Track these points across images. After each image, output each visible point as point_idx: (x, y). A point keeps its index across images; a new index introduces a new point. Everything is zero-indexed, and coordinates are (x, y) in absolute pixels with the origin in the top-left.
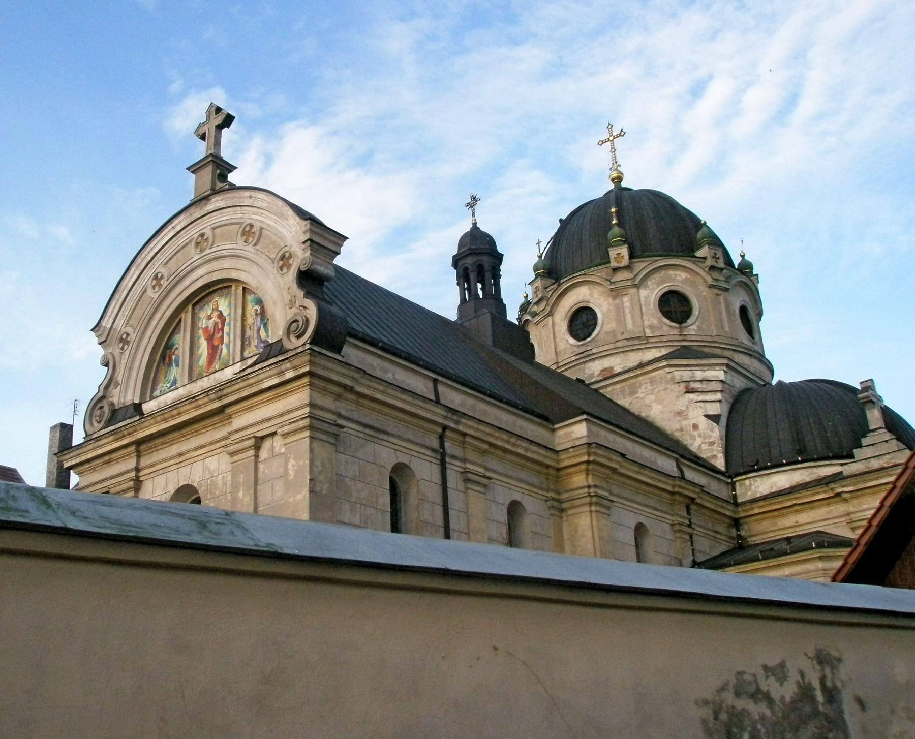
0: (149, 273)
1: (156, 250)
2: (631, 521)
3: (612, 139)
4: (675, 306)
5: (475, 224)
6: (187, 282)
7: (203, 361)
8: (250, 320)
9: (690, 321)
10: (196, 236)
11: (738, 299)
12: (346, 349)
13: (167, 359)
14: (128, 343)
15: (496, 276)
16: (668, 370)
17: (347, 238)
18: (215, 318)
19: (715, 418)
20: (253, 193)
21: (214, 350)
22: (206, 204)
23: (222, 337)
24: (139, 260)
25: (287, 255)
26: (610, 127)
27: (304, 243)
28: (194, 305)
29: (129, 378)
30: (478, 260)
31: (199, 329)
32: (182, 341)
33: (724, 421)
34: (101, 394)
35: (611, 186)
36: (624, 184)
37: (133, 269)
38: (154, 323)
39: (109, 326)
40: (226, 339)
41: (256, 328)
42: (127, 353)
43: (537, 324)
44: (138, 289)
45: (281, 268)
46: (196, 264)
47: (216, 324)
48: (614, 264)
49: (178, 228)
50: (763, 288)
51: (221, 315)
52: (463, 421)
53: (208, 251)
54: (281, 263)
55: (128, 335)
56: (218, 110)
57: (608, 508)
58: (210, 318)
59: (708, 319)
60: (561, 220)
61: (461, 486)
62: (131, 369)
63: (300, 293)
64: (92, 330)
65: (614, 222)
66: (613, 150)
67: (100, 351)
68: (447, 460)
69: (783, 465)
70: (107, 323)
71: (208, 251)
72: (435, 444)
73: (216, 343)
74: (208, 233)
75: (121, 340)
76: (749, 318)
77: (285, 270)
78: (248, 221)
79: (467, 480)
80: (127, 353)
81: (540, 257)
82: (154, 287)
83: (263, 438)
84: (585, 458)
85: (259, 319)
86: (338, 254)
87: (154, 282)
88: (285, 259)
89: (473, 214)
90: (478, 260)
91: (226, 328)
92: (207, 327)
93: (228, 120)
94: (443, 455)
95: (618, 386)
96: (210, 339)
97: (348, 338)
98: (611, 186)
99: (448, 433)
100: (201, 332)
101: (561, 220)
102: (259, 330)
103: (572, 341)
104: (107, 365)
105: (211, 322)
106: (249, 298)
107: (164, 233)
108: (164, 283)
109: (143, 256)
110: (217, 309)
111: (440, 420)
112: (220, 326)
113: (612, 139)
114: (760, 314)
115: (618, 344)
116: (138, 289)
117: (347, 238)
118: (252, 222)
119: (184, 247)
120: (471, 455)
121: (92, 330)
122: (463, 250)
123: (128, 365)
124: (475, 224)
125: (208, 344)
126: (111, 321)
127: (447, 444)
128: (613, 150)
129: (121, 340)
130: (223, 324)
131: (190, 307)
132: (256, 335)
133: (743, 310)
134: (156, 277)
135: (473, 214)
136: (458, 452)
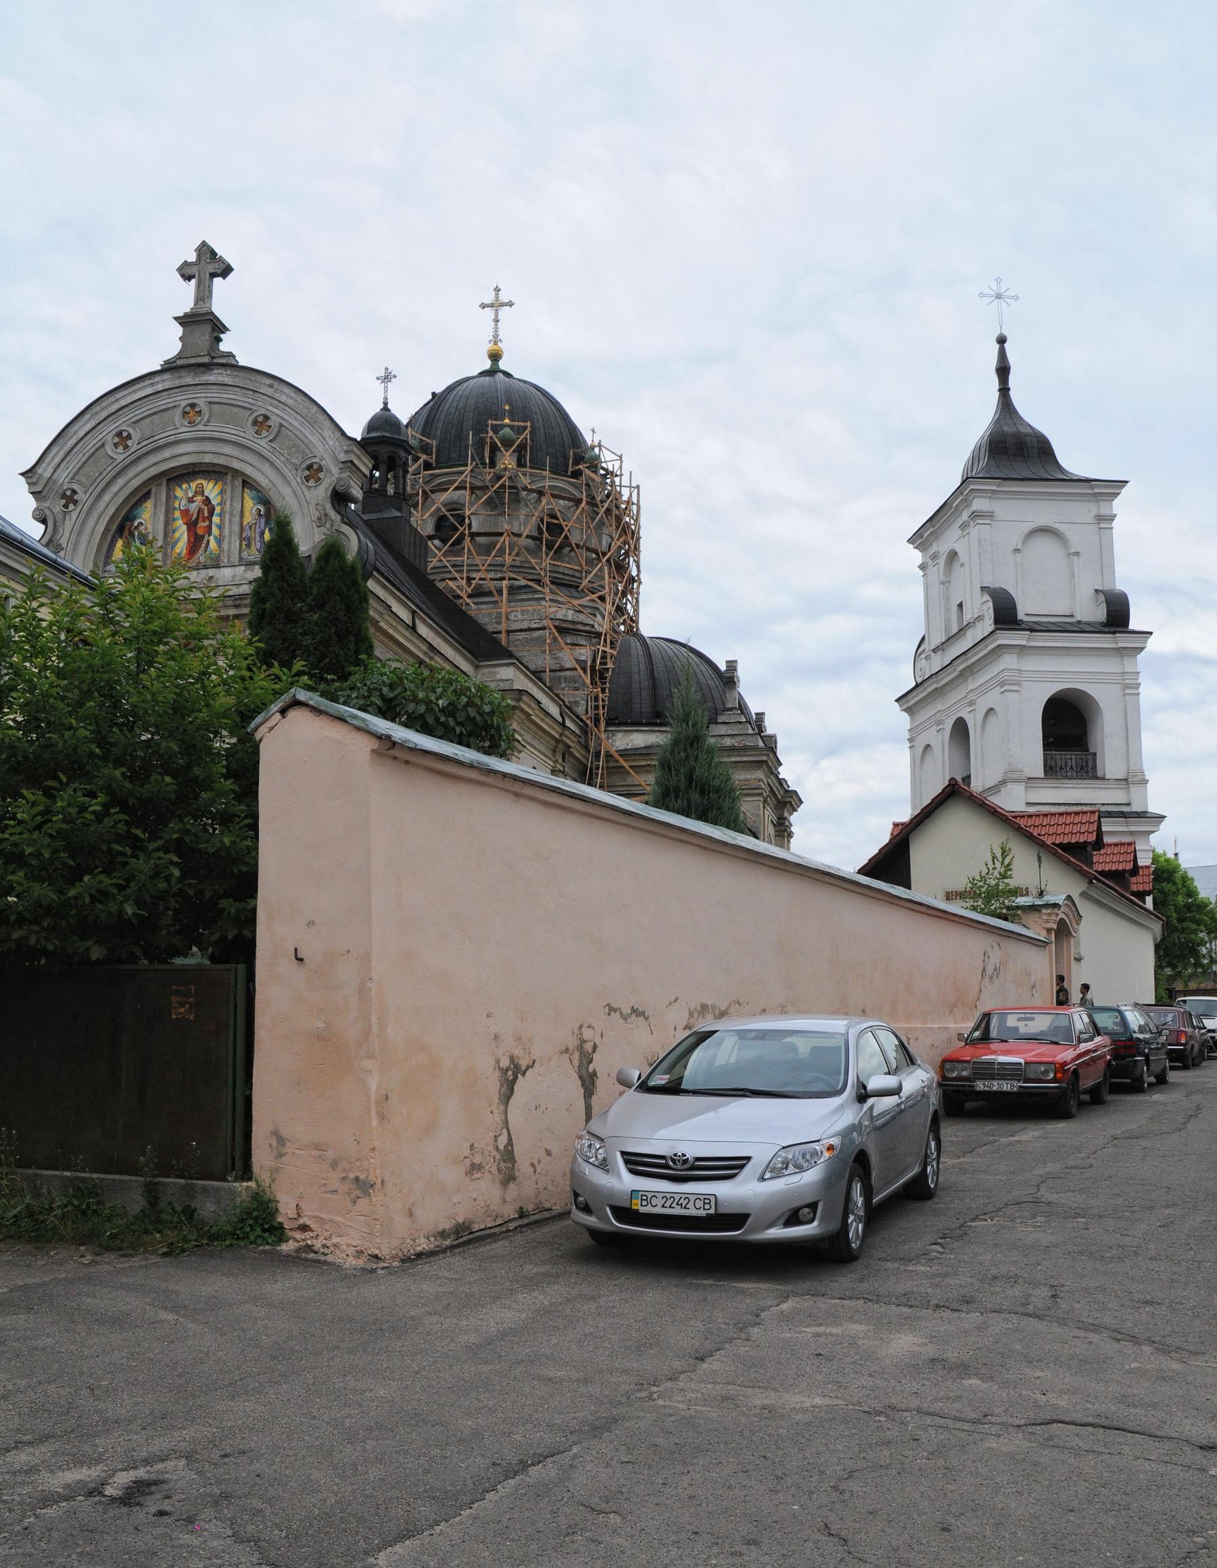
0: (111, 428)
1: (123, 403)
3: (497, 305)
5: (386, 408)
6: (167, 453)
7: (182, 546)
10: (183, 404)
13: (126, 532)
14: (75, 502)
20: (276, 384)
21: (196, 541)
22: (204, 373)
23: (210, 527)
25: (315, 467)
26: (497, 290)
28: (169, 480)
29: (76, 544)
31: (175, 509)
32: (149, 517)
35: (487, 364)
36: (502, 365)
37: (87, 416)
38: (115, 488)
39: (47, 475)
40: (215, 530)
41: (258, 530)
42: (74, 515)
44: (92, 442)
45: (307, 478)
46: (182, 436)
47: (200, 511)
49: (160, 387)
51: (207, 501)
52: (436, 658)
53: (201, 427)
54: (307, 473)
55: (74, 492)
58: (191, 500)
60: (434, 394)
62: (79, 534)
64: (23, 474)
66: (497, 321)
67: (31, 503)
69: (641, 724)
70: (45, 471)
71: (201, 427)
73: (200, 532)
74: (202, 404)
77: (312, 483)
78: (263, 412)
80: (74, 515)
82: (116, 445)
85: (263, 521)
87: (116, 440)
88: (313, 472)
89: (386, 391)
91: (216, 519)
92: (187, 511)
95: (485, 607)
96: (192, 526)
100: (177, 514)
101: (434, 394)
102: (262, 533)
104: (44, 521)
105: (193, 508)
107: (137, 387)
109: (104, 404)
110: (202, 493)
111: (422, 656)
113: (497, 305)
118: (269, 414)
119: (163, 411)
121: (23, 474)
122: (374, 434)
123: (77, 528)
124: (386, 408)
125: (189, 530)
126: (50, 470)
128: (497, 321)
129: (64, 496)
130: (211, 513)
131: (165, 483)
132: (258, 538)
134: (119, 434)
135: (386, 391)
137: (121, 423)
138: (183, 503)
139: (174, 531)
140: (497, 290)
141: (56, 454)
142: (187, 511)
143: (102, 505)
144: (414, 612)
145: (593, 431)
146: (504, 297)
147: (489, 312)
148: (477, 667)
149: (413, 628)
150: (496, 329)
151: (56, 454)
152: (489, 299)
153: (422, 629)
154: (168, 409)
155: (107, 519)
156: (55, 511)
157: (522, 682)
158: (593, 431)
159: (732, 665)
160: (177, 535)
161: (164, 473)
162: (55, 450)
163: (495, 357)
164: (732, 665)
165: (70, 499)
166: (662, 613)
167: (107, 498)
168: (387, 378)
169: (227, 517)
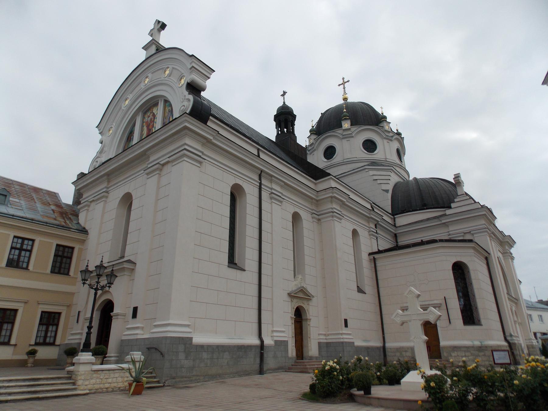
2: (351, 227)
3: (344, 83)
4: (369, 146)
5: (284, 103)
8: (166, 114)
9: (375, 152)
11: (395, 145)
12: (209, 123)
15: (293, 125)
16: (367, 170)
17: (214, 71)
18: (151, 117)
19: (387, 191)
26: (343, 79)
27: (191, 69)
30: (285, 118)
33: (390, 192)
35: (342, 102)
43: (310, 154)
47: (151, 119)
48: (343, 128)
50: (406, 142)
56: (159, 22)
57: (341, 219)
58: (149, 117)
59: (385, 151)
61: (269, 201)
63: (186, 93)
65: (345, 110)
66: (344, 88)
67: (100, 137)
68: (262, 186)
72: (257, 178)
73: (150, 128)
76: (400, 153)
78: (166, 66)
79: (271, 198)
81: (313, 127)
83: (163, 165)
84: (331, 195)
86: (209, 78)
90: (285, 118)
93: (163, 26)
94: (261, 184)
96: (148, 127)
97: (211, 117)
98: (342, 102)
99: (263, 174)
103: (325, 160)
104: (101, 143)
106: (167, 104)
113: (344, 83)
114: (404, 154)
115: (345, 161)
117: (214, 71)
120: (274, 186)
124: (284, 103)
127: (263, 182)
128: (344, 88)
130: (154, 119)
133: (398, 151)
136: (269, 185)
140: (343, 79)
144: (258, 150)
145: (382, 108)
146: (345, 80)
147: (342, 86)
148: (315, 184)
149: (259, 156)
150: (345, 91)
152: (341, 82)
153: (262, 156)
157: (334, 184)
158: (382, 108)
159: (457, 177)
163: (345, 99)
164: (457, 177)
166: (421, 165)
168: (285, 93)
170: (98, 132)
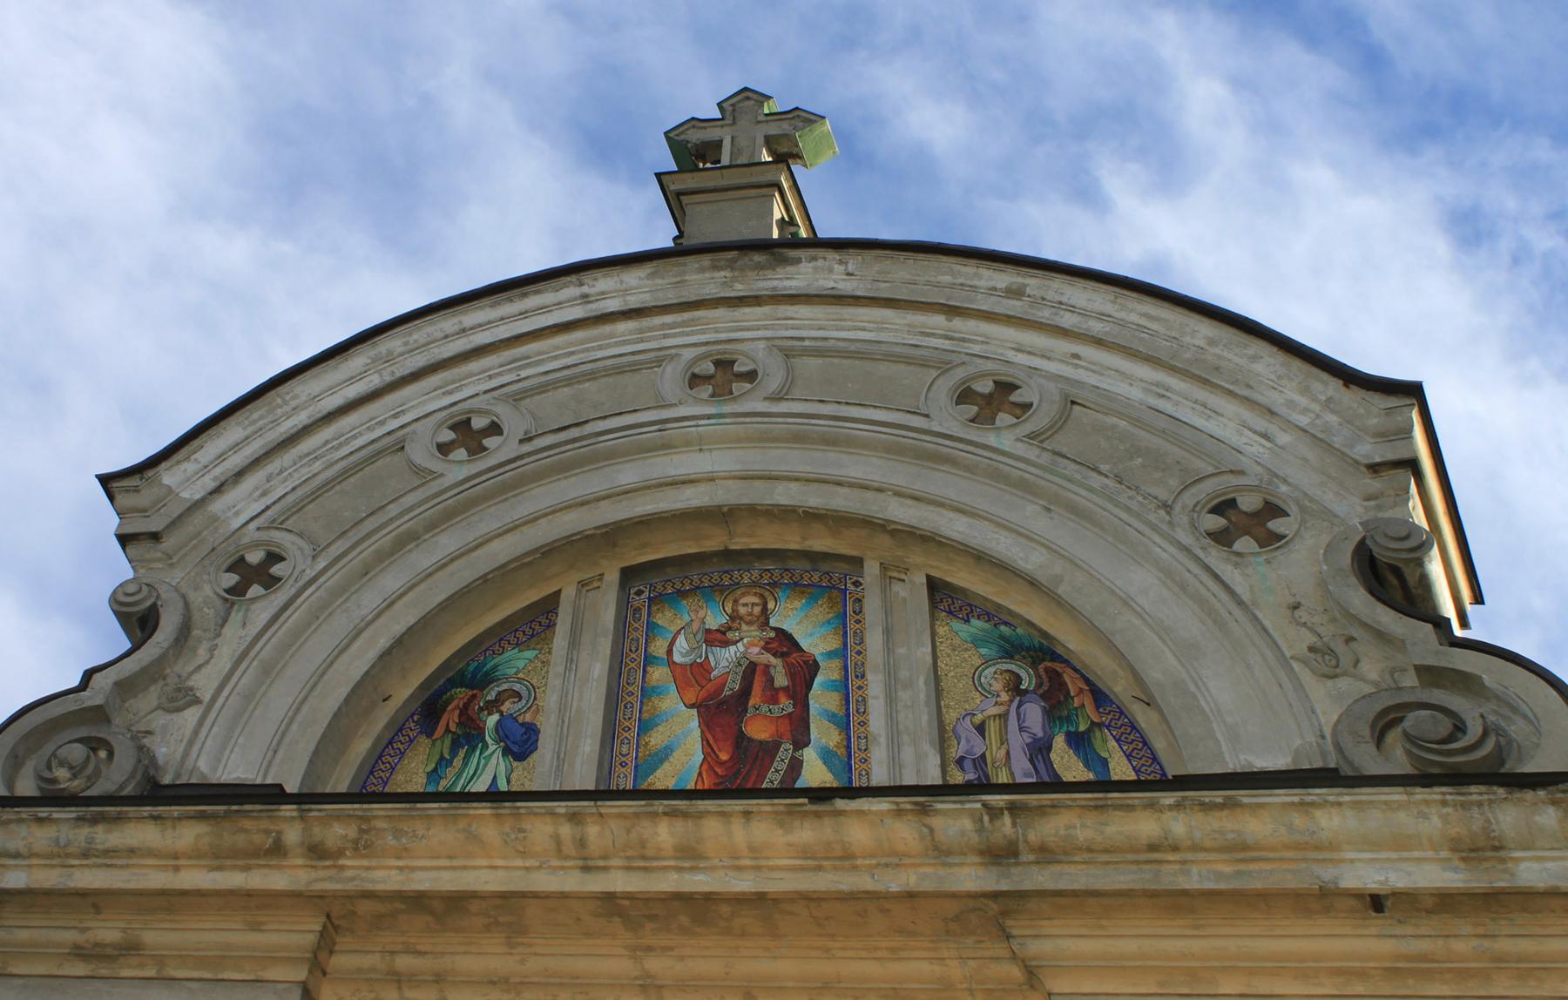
24: (392, 343)
31: (649, 660)
34: (91, 698)
37: (358, 360)
38: (422, 558)
44: (360, 430)
47: (751, 670)
51: (784, 643)
58: (717, 638)
62: (269, 672)
73: (758, 730)
75: (238, 565)
91: (822, 699)
92: (700, 670)
105: (724, 659)
108: (500, 449)
112: (781, 680)
116: (360, 430)
125: (707, 723)
126: (209, 483)
137: (470, 387)
138: (681, 644)
139: (645, 727)
141: (236, 447)
142: (700, 670)
143: (370, 599)
151: (236, 447)
154: (634, 368)
155: (383, 642)
156: (196, 598)
160: (656, 739)
161: (612, 535)
162: (233, 432)
165: (254, 574)
167: (391, 581)
169: (875, 685)
170: (113, 521)
